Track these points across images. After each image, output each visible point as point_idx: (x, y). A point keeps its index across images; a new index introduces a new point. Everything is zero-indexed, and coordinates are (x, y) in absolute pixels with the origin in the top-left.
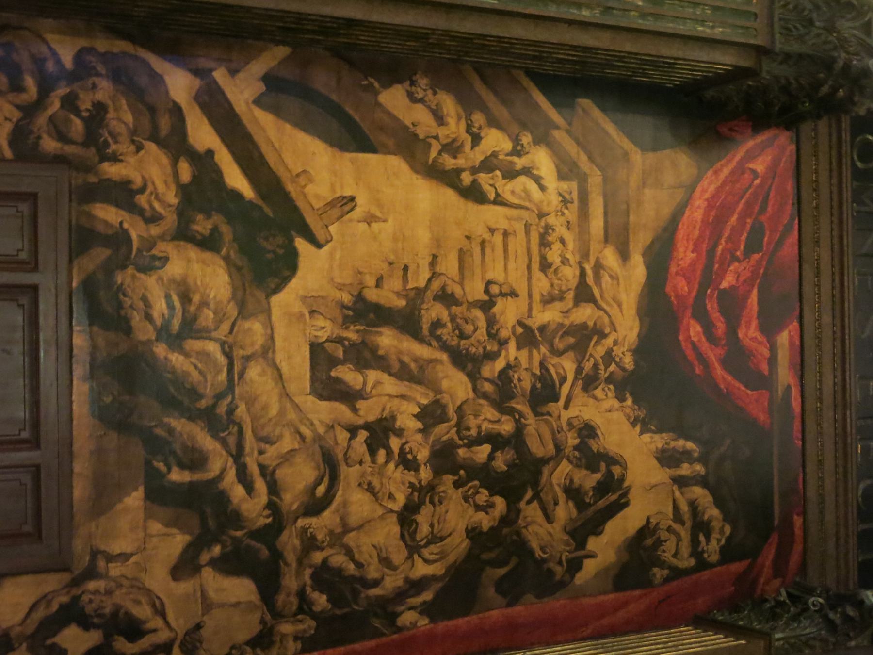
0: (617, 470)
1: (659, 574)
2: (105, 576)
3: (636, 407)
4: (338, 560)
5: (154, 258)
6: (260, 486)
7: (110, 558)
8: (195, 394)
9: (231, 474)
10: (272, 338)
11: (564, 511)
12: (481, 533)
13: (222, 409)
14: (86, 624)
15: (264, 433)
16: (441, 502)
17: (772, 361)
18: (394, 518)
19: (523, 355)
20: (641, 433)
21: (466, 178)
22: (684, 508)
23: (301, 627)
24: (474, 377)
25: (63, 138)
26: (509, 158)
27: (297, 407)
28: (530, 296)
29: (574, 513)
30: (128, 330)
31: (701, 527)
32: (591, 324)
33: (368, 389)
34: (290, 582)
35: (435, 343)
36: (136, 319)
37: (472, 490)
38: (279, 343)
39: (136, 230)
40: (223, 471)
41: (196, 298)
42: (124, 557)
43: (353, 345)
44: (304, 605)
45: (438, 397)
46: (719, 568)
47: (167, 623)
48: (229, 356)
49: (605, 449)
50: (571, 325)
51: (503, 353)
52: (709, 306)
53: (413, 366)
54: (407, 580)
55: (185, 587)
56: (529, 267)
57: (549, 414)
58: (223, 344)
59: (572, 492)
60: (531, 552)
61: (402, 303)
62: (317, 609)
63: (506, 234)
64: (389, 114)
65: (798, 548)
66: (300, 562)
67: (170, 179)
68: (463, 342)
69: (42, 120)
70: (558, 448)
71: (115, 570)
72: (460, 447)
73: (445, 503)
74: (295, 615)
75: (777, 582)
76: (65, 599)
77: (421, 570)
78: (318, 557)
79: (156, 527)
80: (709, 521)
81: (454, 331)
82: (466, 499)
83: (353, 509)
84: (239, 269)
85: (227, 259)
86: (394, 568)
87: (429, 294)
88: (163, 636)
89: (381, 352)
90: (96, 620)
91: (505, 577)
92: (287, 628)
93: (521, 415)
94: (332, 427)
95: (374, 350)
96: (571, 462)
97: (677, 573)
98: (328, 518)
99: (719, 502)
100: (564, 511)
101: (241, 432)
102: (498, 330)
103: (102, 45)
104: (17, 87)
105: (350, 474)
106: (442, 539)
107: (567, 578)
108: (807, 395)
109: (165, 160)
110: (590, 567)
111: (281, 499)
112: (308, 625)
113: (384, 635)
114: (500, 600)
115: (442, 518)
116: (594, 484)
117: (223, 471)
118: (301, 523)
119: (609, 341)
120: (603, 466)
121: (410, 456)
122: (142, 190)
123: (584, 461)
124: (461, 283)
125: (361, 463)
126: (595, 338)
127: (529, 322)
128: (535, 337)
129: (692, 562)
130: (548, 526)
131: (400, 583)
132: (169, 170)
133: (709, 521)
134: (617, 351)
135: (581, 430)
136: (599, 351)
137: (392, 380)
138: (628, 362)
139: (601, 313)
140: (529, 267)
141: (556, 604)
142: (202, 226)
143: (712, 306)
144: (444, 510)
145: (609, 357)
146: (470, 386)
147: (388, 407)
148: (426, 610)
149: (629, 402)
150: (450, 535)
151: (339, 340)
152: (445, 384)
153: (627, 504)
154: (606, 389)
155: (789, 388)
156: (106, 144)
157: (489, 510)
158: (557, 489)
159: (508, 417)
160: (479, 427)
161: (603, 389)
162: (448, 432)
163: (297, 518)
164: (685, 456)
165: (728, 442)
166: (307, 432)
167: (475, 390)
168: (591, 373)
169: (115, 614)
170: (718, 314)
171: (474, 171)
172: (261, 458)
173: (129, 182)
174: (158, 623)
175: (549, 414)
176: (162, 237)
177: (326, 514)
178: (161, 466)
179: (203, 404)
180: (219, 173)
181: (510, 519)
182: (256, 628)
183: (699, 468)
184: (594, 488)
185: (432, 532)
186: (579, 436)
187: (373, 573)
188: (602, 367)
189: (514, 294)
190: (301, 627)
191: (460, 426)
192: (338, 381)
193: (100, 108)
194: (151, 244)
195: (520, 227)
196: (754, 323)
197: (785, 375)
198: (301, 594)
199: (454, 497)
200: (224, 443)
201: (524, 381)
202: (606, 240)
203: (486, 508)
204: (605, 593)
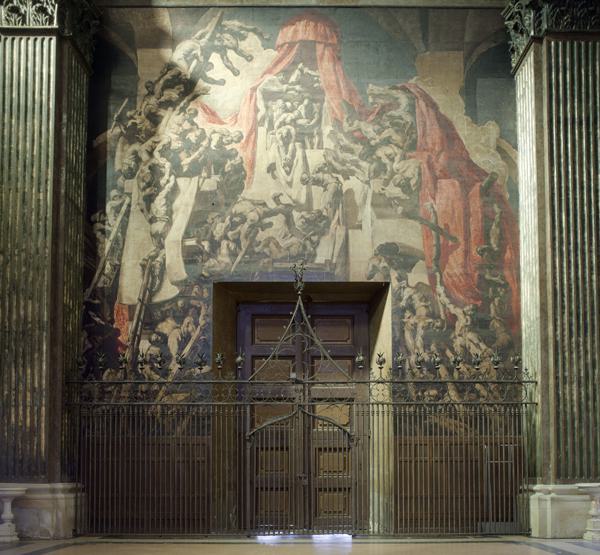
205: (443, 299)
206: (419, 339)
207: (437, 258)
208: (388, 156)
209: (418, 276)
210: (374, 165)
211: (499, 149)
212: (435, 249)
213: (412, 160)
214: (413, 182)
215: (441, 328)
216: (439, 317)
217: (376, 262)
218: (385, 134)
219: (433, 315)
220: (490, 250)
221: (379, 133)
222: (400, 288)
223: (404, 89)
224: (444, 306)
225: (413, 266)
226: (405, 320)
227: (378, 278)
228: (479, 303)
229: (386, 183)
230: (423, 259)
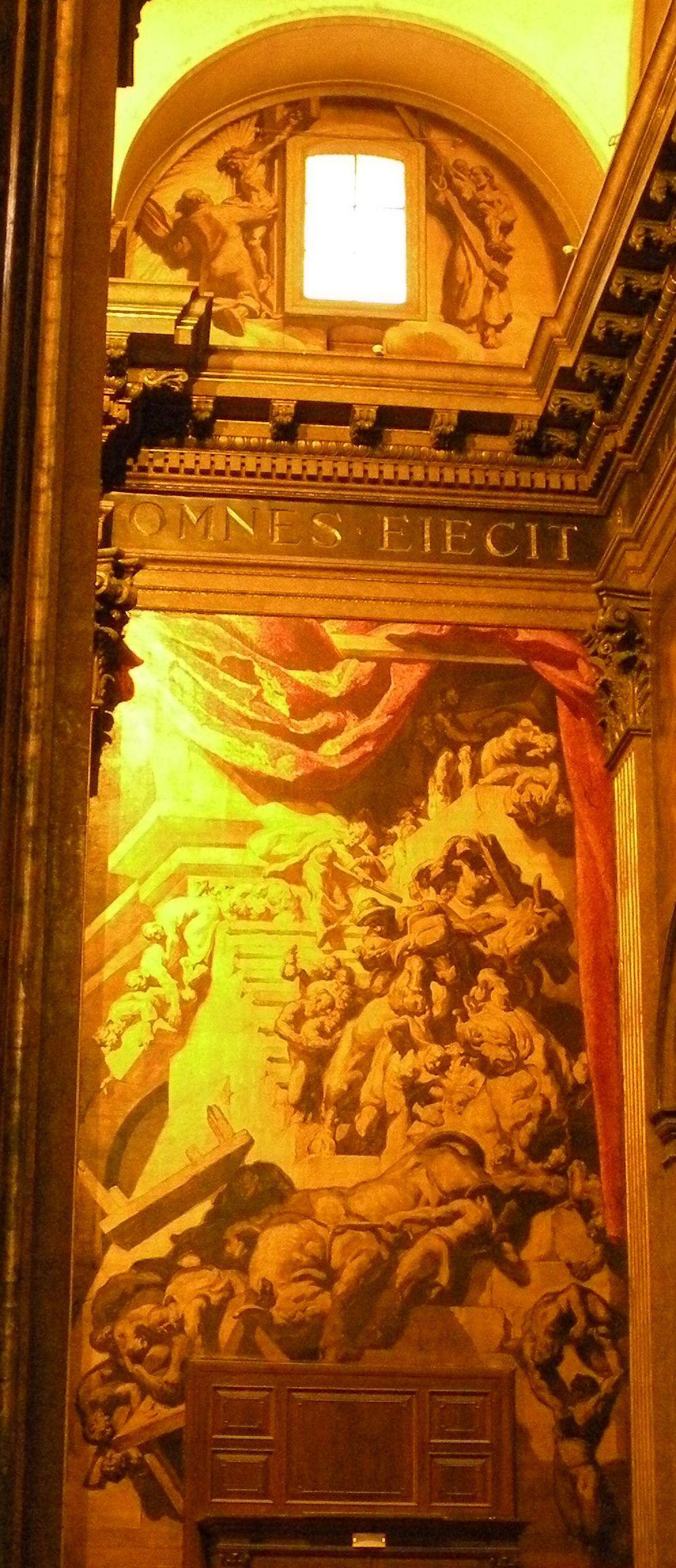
0: (461, 848)
1: (561, 807)
2: (522, 1339)
3: (402, 821)
4: (523, 1136)
5: (263, 1291)
6: (456, 1205)
7: (507, 1337)
8: (376, 1260)
9: (445, 1231)
10: (330, 1189)
11: (496, 907)
12: (510, 996)
13: (389, 1236)
14: (558, 1358)
15: (411, 1200)
16: (480, 1035)
17: (362, 657)
18: (490, 1081)
19: (351, 943)
20: (427, 817)
21: (189, 994)
22: (501, 772)
23: (577, 1173)
24: (369, 996)
25: (166, 1363)
26: (168, 947)
27: (390, 1170)
28: (297, 933)
29: (498, 896)
30: (322, 1317)
31: (520, 755)
32: (323, 869)
33: (377, 1101)
34: (539, 1181)
35: (338, 1034)
36: (313, 1307)
37: (471, 1003)
38: (337, 1184)
39: (240, 1305)
40: (441, 1238)
41: (296, 1255)
42: (507, 1325)
43: (338, 1114)
44: (559, 1170)
45: (386, 1034)
46: (562, 735)
47: (563, 1292)
48: (345, 1229)
49: (440, 860)
50: (324, 891)
51: (348, 964)
52: (305, 731)
53: (358, 1057)
54: (546, 1072)
55: (535, 1273)
56: (269, 933)
57: (405, 919)
58: (335, 1234)
59: (479, 898)
60: (532, 945)
61: (302, 1064)
62: (563, 1158)
63: (238, 956)
64: (132, 1069)
65: (549, 637)
66: (523, 1172)
67: (198, 1274)
68: (337, 1006)
69: (152, 1380)
70: (438, 910)
71: (517, 1333)
72: (431, 1014)
73: (480, 1030)
74: (567, 1178)
75: (582, 666)
76: (537, 1375)
77: (538, 1059)
78: (520, 1156)
79: (484, 1298)
80: (517, 744)
81: (327, 1014)
82: (479, 1010)
83: (480, 1121)
84: (272, 1216)
85: (263, 1228)
86: (535, 1084)
87: (294, 1037)
88: (573, 1295)
89: (345, 1088)
90: (556, 1351)
91: (551, 972)
92: (577, 1187)
93: (405, 949)
94: (409, 1137)
95: (343, 1095)
96: (451, 898)
97: (563, 785)
99: (498, 731)
100: (496, 907)
101: (411, 1221)
102: (327, 968)
103: (87, 1328)
104: (125, 1400)
106: (513, 1036)
107: (557, 907)
108: (397, 617)
109: (181, 1278)
110: (551, 883)
111: (469, 1186)
112: (576, 1167)
113: (591, 1097)
114: (570, 982)
115: (494, 1034)
116: (473, 873)
117: (441, 1238)
118: (489, 1170)
119: (341, 851)
120: (456, 862)
121: (438, 1064)
122: (207, 1298)
123: (451, 883)
124: (285, 1005)
125: (441, 1112)
126: (336, 864)
127: (320, 936)
128: (333, 930)
129: (554, 766)
130: (508, 926)
131: (547, 1080)
132: (191, 1275)
133: (517, 744)
134: (349, 841)
135: (421, 885)
136: (348, 863)
137: (370, 1076)
138: (360, 828)
139: (312, 856)
140: (269, 933)
141: (581, 922)
142: (235, 1248)
144: (487, 1033)
145: (354, 850)
146: (376, 1001)
147: (392, 1082)
148: (573, 1054)
149: (395, 829)
150: (510, 1029)
151: (334, 1126)
152: (375, 1025)
153: (494, 839)
154: (384, 855)
155: (390, 638)
156: (170, 1327)
157: (490, 987)
158: (474, 915)
159: (407, 963)
160: (415, 993)
161: (384, 858)
162: (418, 1025)
163: (485, 1173)
164: (452, 765)
165: (440, 716)
166: (412, 1161)
167: (380, 995)
168: (368, 871)
169: (553, 1335)
170: (315, 720)
171: (181, 986)
172: (433, 1201)
173: (200, 1308)
174: (562, 1300)
175: (405, 919)
176: (246, 1284)
177: (483, 1147)
178: (435, 1291)
179: (385, 1254)
180: (189, 1232)
182: (575, 1214)
183: (465, 751)
184: (477, 874)
185: (506, 1045)
186: (427, 887)
187: (537, 1105)
188: (363, 859)
189: (294, 951)
190: (577, 1173)
192: (369, 1129)
193: (140, 1332)
194: (250, 1292)
195: (232, 940)
196: (324, 676)
197: (376, 642)
198: (552, 1172)
199: (476, 1022)
200: (418, 1236)
201: (374, 944)
202: (243, 846)
203: (488, 989)
204: (575, 868)
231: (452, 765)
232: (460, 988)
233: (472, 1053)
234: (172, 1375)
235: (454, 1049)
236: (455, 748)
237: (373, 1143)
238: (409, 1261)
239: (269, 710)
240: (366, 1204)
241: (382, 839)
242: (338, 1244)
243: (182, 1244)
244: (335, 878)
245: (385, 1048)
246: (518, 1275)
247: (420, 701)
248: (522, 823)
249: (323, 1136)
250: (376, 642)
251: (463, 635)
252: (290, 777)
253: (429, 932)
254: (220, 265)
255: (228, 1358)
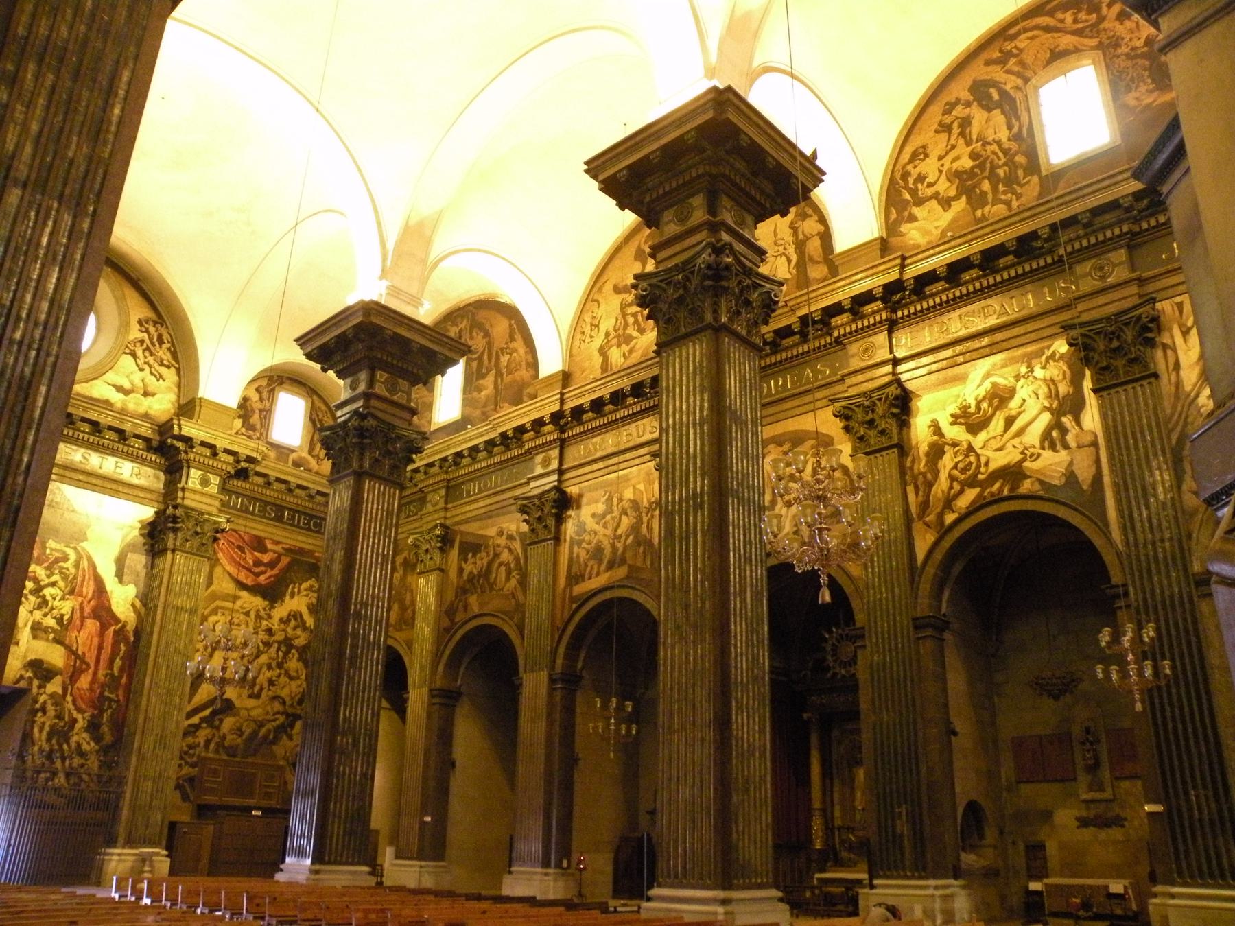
4: (297, 698)
11: (299, 632)
17: (274, 552)
22: (305, 593)
24: (262, 653)
25: (193, 755)
39: (216, 739)
55: (295, 737)
59: (295, 628)
98: (287, 699)
99: (307, 581)
100: (299, 632)
105: (279, 693)
136: (262, 613)
138: (267, 603)
142: (217, 723)
143: (257, 570)
145: (264, 609)
164: (293, 588)
181: (297, 649)
191: (273, 659)
193: (187, 745)
201: (265, 637)
203: (293, 655)
205: (70, 705)
206: (45, 733)
207: (71, 677)
208: (51, 596)
209: (54, 686)
210: (40, 600)
211: (133, 605)
212: (71, 669)
213: (68, 602)
214: (66, 618)
215: (64, 727)
216: (64, 719)
217: (23, 672)
218: (53, 579)
219: (59, 717)
220: (112, 675)
221: (48, 577)
222: (38, 694)
223: (75, 549)
224: (70, 711)
225: (52, 678)
226: (37, 719)
227: (22, 684)
228: (96, 712)
229: (45, 615)
230: (61, 674)
231: (293, 588)
232: (286, 654)
233: (287, 674)
234: (195, 759)
235: (283, 671)
236: (295, 584)
237: (258, 696)
238: (263, 731)
239: (248, 563)
240: (253, 713)
241: (272, 607)
242: (245, 724)
243: (203, 720)
244: (258, 616)
245: (265, 669)
246: (290, 738)
247: (289, 567)
248: (309, 609)
249: (245, 692)
250: (278, 548)
251: (301, 551)
252: (250, 584)
253: (280, 636)
254: (251, 420)
255: (211, 755)
